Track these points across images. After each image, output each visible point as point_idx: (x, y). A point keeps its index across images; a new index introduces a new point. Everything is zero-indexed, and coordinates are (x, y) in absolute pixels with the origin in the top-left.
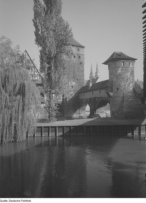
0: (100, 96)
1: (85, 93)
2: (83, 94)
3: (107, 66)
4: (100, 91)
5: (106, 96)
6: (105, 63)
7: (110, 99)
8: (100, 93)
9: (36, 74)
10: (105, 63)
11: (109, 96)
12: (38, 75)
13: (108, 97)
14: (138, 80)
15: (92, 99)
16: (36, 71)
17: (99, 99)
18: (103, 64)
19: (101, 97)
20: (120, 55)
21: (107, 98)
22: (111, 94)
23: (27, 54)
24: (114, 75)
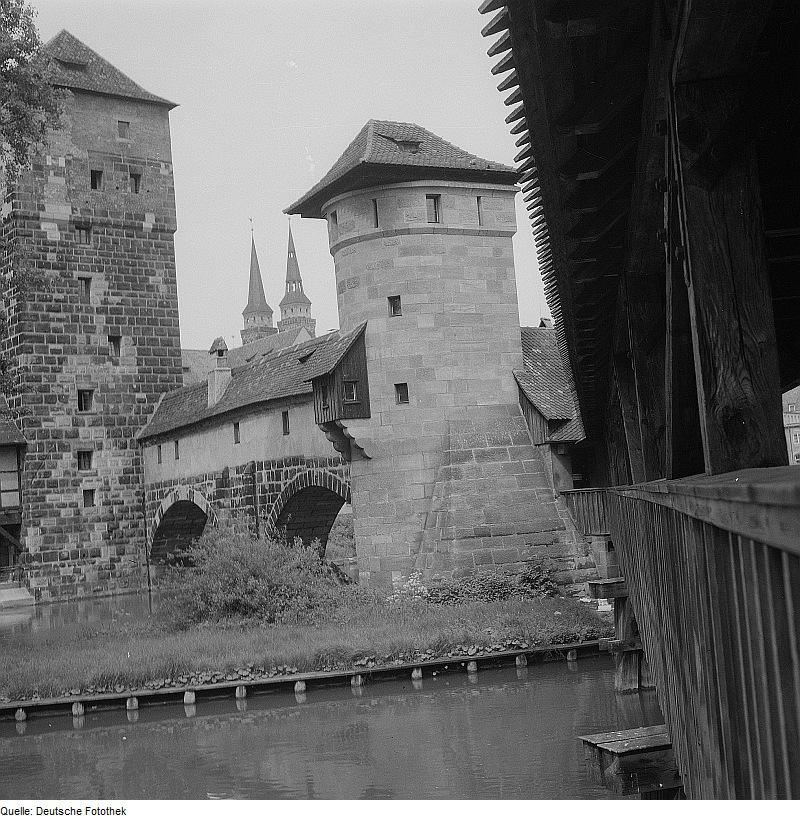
0: (288, 453)
1: (182, 436)
2: (168, 447)
3: (319, 227)
4: (285, 415)
5: (326, 447)
6: (310, 207)
7: (357, 467)
8: (286, 432)
10: (310, 207)
11: (348, 448)
13: (340, 455)
14: (543, 324)
15: (233, 475)
17: (278, 479)
18: (291, 211)
19: (296, 461)
20: (412, 145)
21: (336, 462)
22: (354, 429)
24: (373, 293)
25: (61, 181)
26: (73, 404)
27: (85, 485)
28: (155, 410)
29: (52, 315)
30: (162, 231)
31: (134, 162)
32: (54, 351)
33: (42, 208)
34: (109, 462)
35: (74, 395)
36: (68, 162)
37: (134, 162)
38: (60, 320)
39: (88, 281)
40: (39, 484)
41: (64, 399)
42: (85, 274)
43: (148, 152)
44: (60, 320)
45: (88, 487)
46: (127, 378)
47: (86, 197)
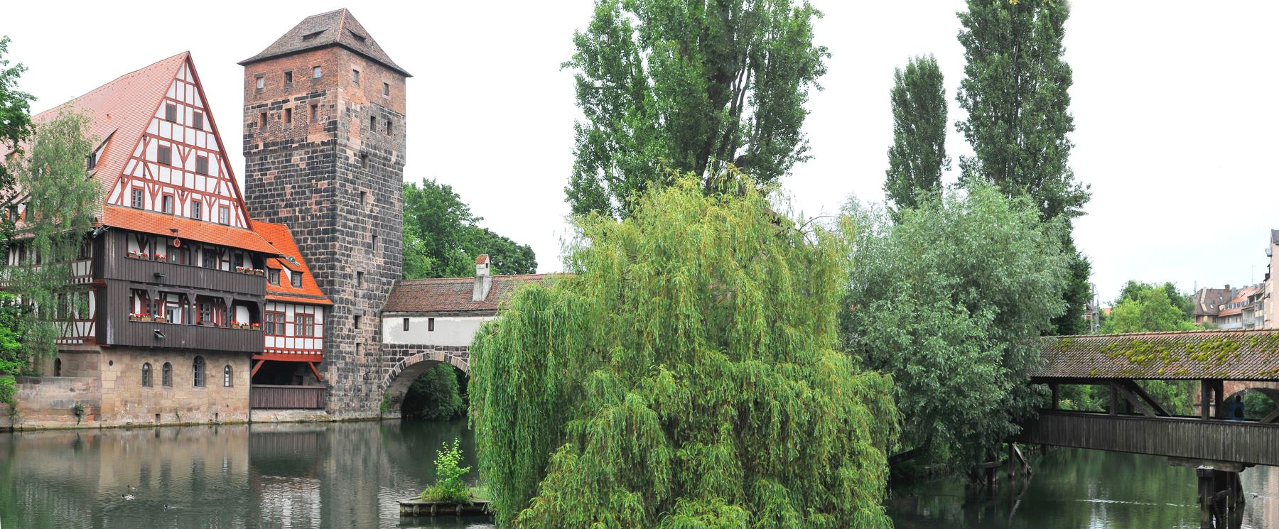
9: (224, 192)
12: (230, 199)
16: (224, 179)
23: (190, 79)
25: (358, 121)
26: (355, 282)
27: (357, 340)
28: (390, 291)
29: (349, 216)
30: (399, 164)
31: (390, 113)
32: (349, 243)
33: (348, 139)
34: (367, 325)
35: (355, 274)
36: (361, 108)
37: (390, 113)
38: (352, 221)
39: (363, 193)
40: (338, 335)
41: (351, 277)
42: (364, 189)
43: (396, 108)
44: (352, 221)
45: (359, 342)
46: (378, 267)
47: (368, 134)
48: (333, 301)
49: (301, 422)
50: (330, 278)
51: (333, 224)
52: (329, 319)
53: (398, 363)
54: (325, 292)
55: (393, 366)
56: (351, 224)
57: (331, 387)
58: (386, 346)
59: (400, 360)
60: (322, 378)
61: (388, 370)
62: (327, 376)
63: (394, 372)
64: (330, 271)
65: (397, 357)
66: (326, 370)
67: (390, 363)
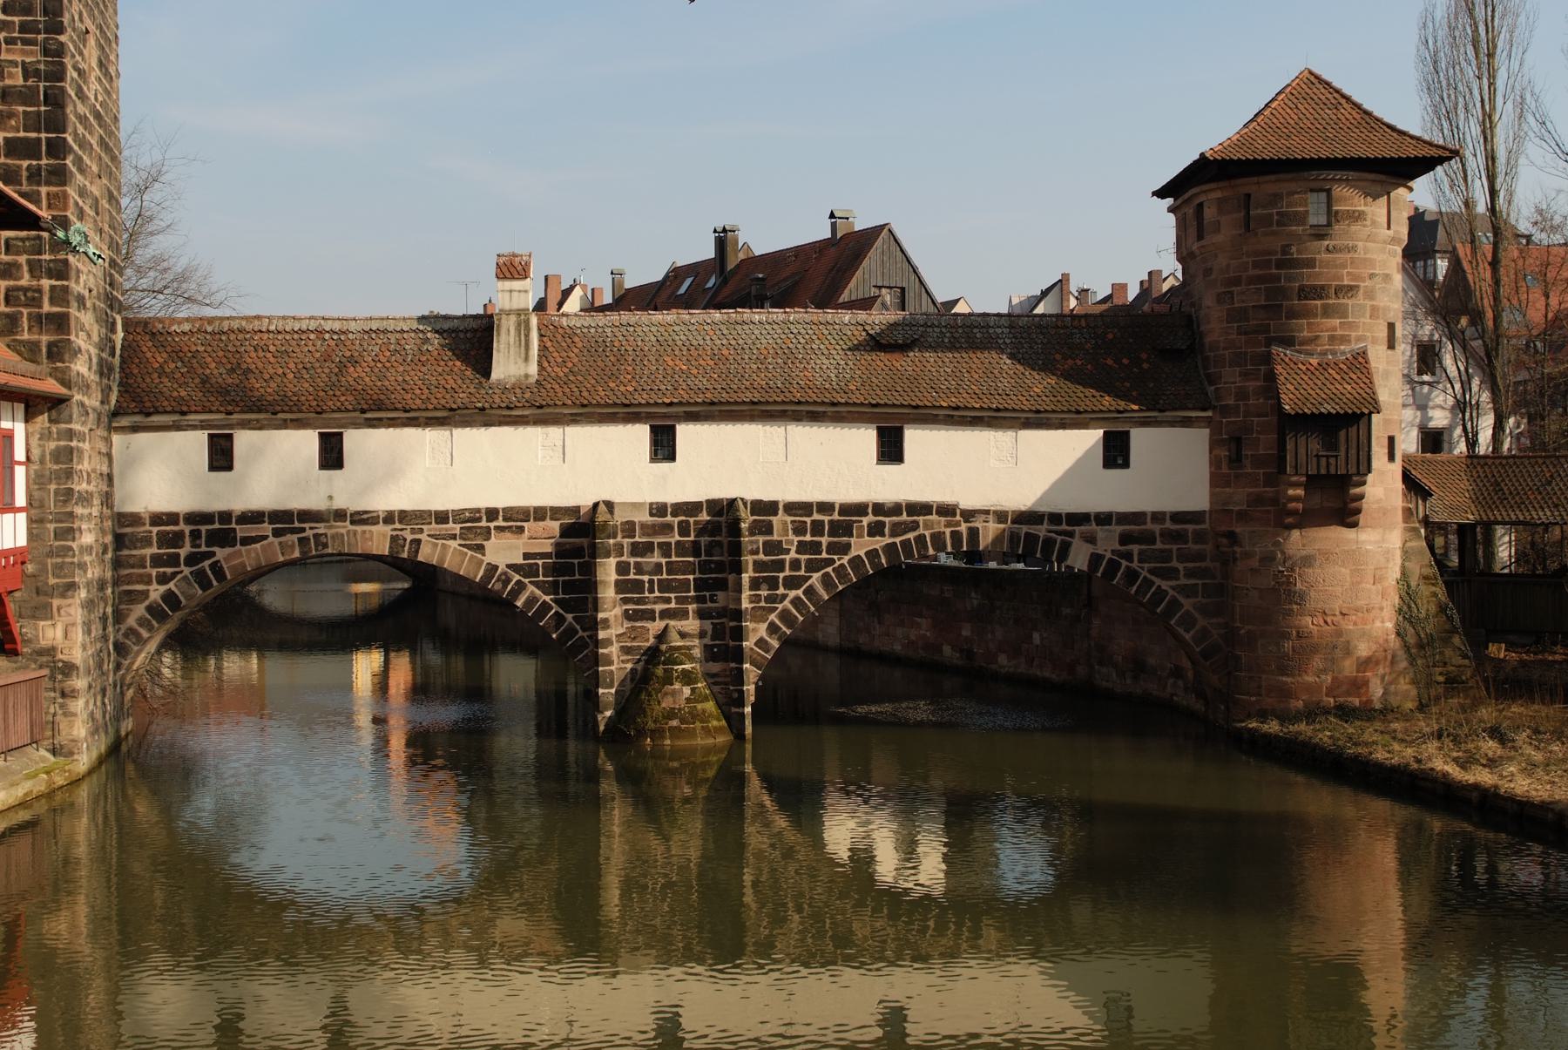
28: (118, 352)
48: (66, 383)
49: (23, 805)
50: (47, 307)
51: (56, 122)
52: (52, 445)
53: (187, 571)
54: (30, 352)
55: (163, 580)
56: (81, 130)
57: (69, 669)
58: (135, 519)
59: (192, 560)
60: (28, 642)
61: (146, 594)
62: (50, 633)
63: (169, 597)
64: (46, 283)
65: (183, 552)
66: (42, 611)
67: (154, 572)
